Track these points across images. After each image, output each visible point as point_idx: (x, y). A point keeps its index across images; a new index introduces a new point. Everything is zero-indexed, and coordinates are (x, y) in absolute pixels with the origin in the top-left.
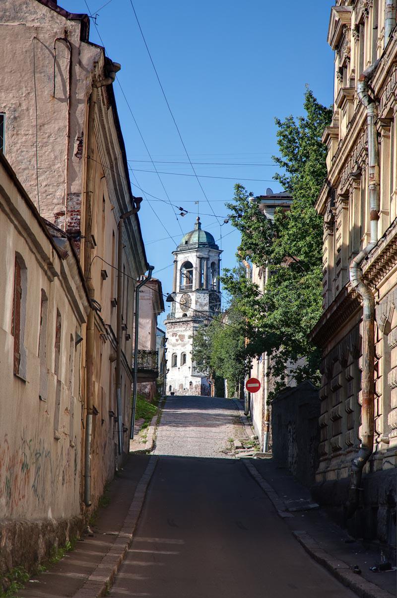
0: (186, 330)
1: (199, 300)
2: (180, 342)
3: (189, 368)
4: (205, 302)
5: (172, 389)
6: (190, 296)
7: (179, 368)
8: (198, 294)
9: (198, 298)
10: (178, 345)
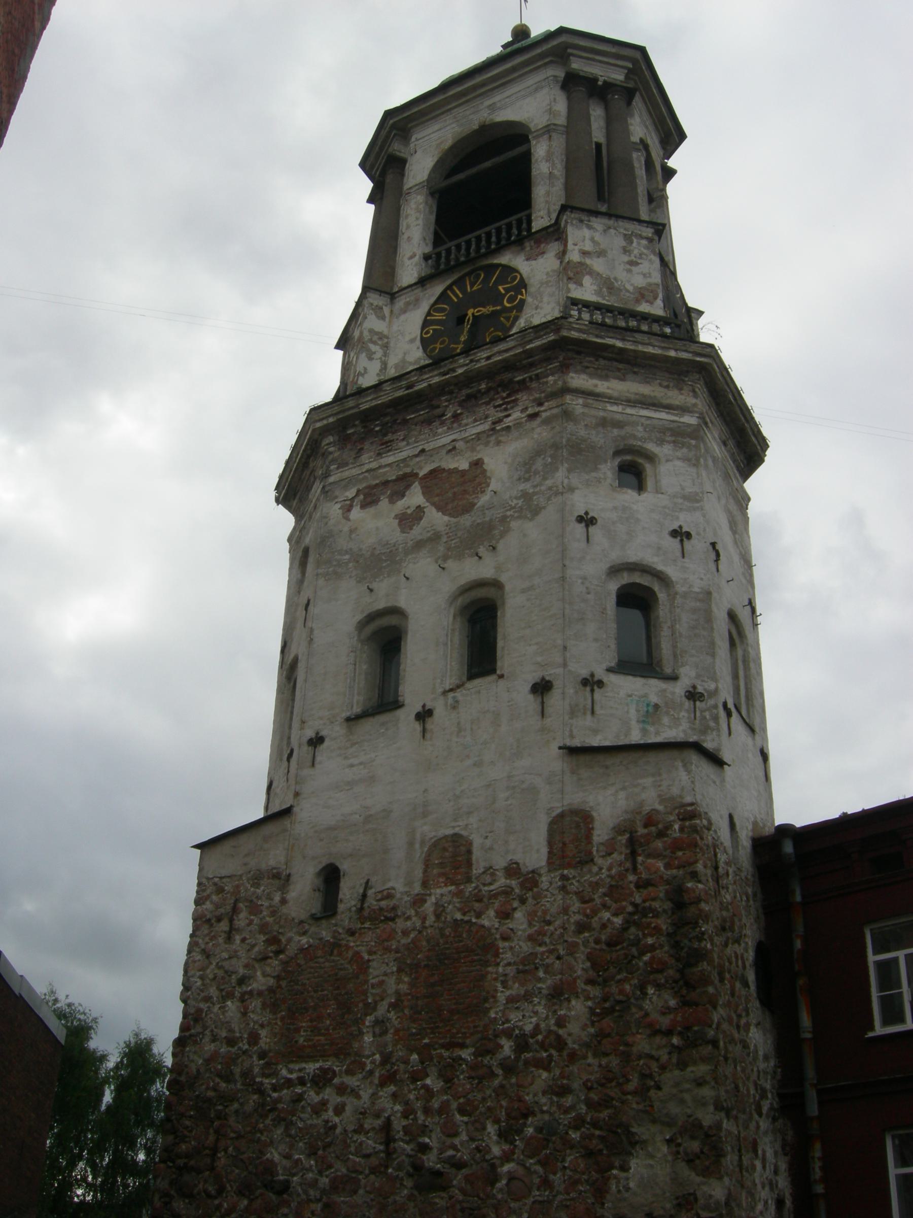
0: (497, 433)
1: (597, 265)
2: (435, 519)
3: (542, 688)
4: (639, 281)
5: (348, 892)
6: (509, 270)
7: (424, 715)
8: (586, 233)
9: (584, 253)
10: (419, 545)
